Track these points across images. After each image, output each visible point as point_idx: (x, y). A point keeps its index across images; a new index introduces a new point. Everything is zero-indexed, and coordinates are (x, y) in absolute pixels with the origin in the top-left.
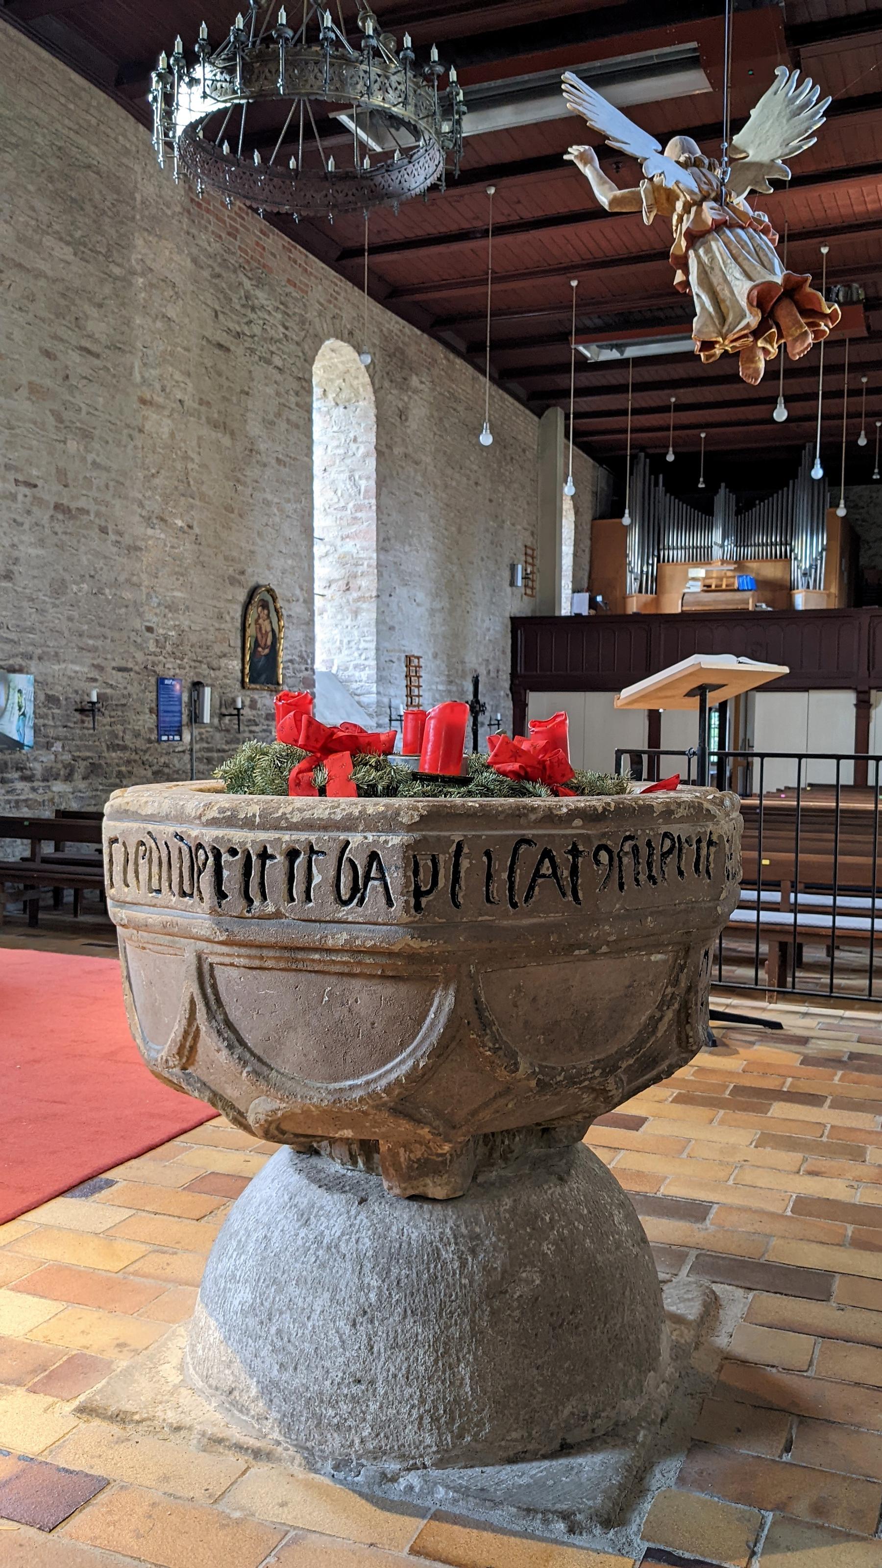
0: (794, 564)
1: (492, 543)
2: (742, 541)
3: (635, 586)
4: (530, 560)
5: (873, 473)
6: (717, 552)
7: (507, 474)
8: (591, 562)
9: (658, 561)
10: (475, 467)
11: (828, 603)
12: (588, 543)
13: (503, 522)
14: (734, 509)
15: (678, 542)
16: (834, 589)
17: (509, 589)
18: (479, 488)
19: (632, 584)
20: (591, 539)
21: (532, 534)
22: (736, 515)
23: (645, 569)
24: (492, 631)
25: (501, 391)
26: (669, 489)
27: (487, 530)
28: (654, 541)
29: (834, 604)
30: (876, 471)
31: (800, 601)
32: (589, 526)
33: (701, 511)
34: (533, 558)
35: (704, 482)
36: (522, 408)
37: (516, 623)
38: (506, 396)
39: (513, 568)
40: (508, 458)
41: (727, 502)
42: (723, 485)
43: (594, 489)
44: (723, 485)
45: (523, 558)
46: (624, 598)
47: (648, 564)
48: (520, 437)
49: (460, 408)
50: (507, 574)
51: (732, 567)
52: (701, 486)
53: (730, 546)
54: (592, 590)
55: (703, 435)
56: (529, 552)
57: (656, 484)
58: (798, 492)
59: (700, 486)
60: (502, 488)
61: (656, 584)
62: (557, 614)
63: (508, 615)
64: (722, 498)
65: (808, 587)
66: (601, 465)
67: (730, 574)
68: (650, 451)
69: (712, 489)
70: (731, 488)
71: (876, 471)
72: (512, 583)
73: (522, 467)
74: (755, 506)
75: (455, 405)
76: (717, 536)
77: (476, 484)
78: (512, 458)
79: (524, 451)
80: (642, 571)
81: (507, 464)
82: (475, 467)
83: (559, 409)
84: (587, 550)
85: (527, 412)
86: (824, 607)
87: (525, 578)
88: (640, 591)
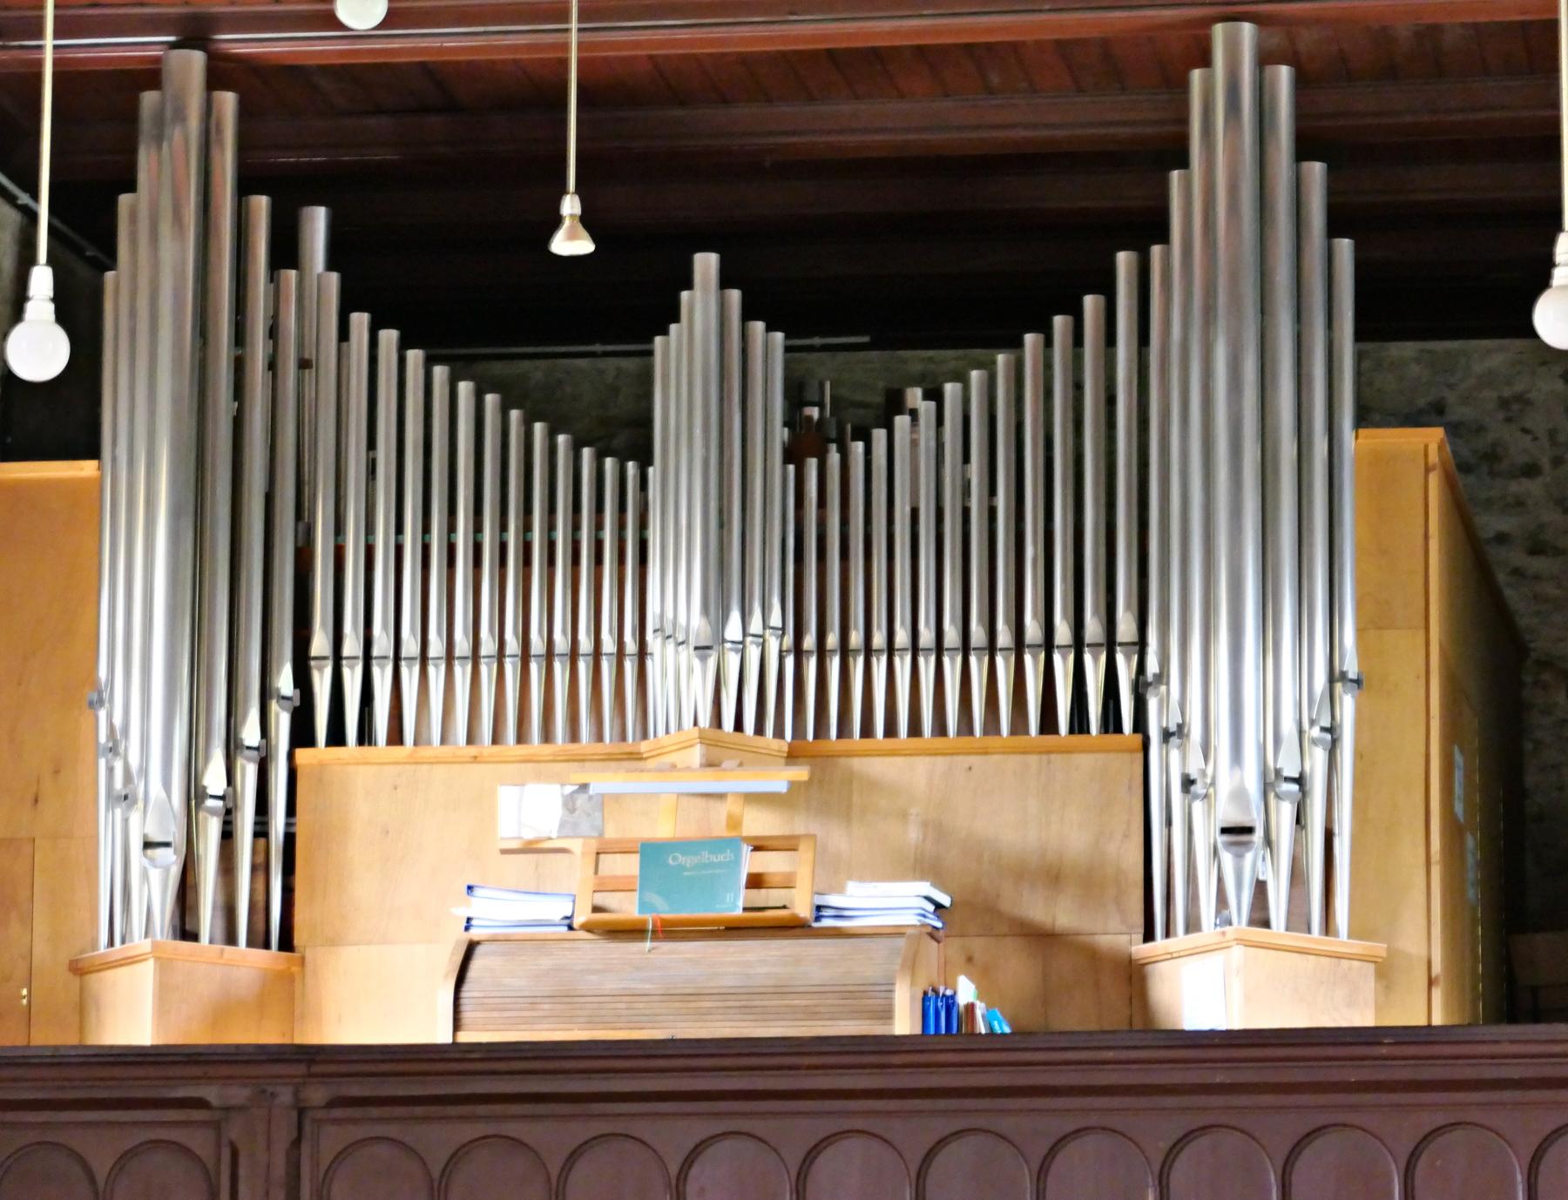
0: (1167, 764)
3: (154, 887)
6: (680, 683)
9: (302, 735)
11: (1379, 1008)
14: (781, 434)
15: (411, 620)
22: (793, 454)
23: (214, 779)
28: (266, 584)
29: (1423, 1005)
31: (1210, 986)
35: (589, 221)
42: (706, 264)
44: (706, 264)
47: (232, 746)
51: (778, 780)
52: (571, 243)
53: (761, 635)
57: (286, 252)
61: (268, 888)
65: (1261, 919)
67: (759, 823)
68: (236, 42)
69: (631, 299)
80: (195, 794)
88: (186, 931)
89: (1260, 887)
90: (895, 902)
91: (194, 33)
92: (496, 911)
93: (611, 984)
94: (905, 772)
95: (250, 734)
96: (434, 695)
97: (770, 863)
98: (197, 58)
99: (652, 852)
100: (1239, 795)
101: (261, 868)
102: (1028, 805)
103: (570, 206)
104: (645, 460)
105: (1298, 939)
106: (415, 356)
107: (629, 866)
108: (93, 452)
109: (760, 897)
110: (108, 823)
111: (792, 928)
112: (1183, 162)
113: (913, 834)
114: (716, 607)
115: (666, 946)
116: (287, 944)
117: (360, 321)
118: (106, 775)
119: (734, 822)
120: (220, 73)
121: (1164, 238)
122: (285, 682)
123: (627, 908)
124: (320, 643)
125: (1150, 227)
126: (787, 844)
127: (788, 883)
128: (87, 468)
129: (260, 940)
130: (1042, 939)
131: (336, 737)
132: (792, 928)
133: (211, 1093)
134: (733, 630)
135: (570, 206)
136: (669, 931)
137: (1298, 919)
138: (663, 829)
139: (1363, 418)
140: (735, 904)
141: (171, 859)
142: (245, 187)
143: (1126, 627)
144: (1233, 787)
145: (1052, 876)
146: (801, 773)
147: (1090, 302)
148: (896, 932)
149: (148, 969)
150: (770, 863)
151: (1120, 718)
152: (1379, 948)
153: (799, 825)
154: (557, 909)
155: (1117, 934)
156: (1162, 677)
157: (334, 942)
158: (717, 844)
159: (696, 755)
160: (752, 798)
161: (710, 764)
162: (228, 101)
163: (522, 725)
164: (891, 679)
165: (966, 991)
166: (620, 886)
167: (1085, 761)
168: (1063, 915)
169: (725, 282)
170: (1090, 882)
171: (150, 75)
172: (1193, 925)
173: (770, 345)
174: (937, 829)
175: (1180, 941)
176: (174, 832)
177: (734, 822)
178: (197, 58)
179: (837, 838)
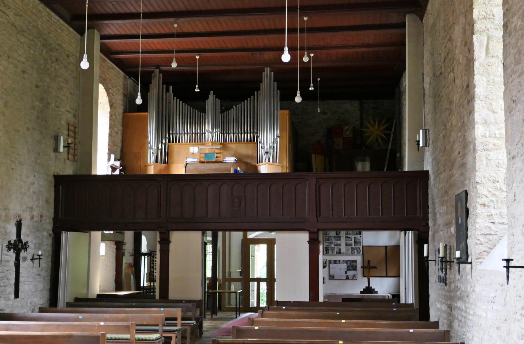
0: (259, 146)
1: (38, 118)
2: (224, 130)
3: (153, 158)
4: (72, 134)
5: (310, 86)
6: (209, 137)
7: (53, 69)
8: (123, 141)
9: (169, 142)
10: (22, 59)
12: (121, 128)
13: (48, 104)
14: (220, 110)
16: (286, 163)
17: (53, 154)
18: (26, 76)
19: (151, 155)
20: (123, 126)
21: (75, 116)
22: (221, 113)
23: (160, 146)
24: (36, 185)
25: (48, 10)
26: (176, 94)
27: (33, 108)
29: (286, 170)
30: (312, 85)
31: (264, 169)
32: (121, 116)
33: (196, 104)
34: (75, 133)
35: (199, 88)
36: (66, 25)
37: (60, 182)
38: (53, 14)
39: (56, 139)
40: (54, 59)
41: (214, 104)
42: (212, 92)
43: (126, 93)
44: (212, 92)
45: (66, 132)
46: (146, 166)
47: (162, 143)
48: (64, 46)
49: (10, 13)
50: (52, 143)
52: (197, 90)
53: (217, 132)
54: (121, 158)
55: (197, 57)
56: (71, 128)
57: (168, 90)
58: (261, 98)
59: (196, 90)
60: (47, 79)
61: (166, 157)
62: (93, 173)
63: (52, 175)
64: (211, 101)
65: (269, 161)
66: (130, 77)
67: (217, 151)
69: (203, 96)
70: (218, 96)
71: (312, 85)
72: (56, 150)
73: (66, 67)
74: (232, 107)
75: (4, 9)
76: (208, 127)
77: (24, 72)
78: (57, 60)
79: (68, 56)
80: (158, 148)
81: (53, 62)
82: (22, 59)
83: (96, 31)
84: (120, 133)
85: (71, 29)
86: (280, 172)
87: (67, 146)
88: (157, 161)
89: (269, 158)
90: (231, 159)
91: (158, 67)
92: (189, 160)
93: (201, 168)
94: (233, 146)
95: (164, 142)
96: (183, 138)
97: (218, 155)
98: (158, 70)
99: (206, 154)
100: (267, 148)
101: (165, 156)
102: (245, 150)
103: (197, 86)
104: (205, 113)
105: (273, 164)
106: (181, 102)
107: (203, 155)
108: (147, 112)
109: (217, 159)
110: (149, 151)
111: (220, 162)
112: (262, 82)
113: (233, 152)
114: (213, 129)
115: (207, 164)
116: (167, 163)
117: (175, 98)
118: (148, 146)
119: (214, 151)
120: (161, 71)
121: (260, 90)
122: (167, 136)
123: (203, 160)
124: (171, 132)
125: (258, 89)
126: (220, 153)
127: (220, 157)
128: (146, 113)
129: (165, 163)
130: (247, 164)
131: (173, 142)
132: (220, 162)
133: (158, 179)
134: (214, 131)
135: (197, 86)
136: (208, 162)
137: (273, 161)
138: (207, 152)
139: (281, 109)
140: (214, 160)
141: (155, 154)
142: (163, 84)
143: (255, 131)
144: (267, 147)
145: (248, 157)
146: (221, 146)
147: (252, 97)
148: (231, 163)
149: (153, 166)
150: (218, 155)
151: (255, 142)
152: (281, 164)
153: (221, 151)
154: (196, 160)
155: (254, 163)
156: (259, 136)
157: (173, 163)
158: (213, 153)
159: (210, 144)
160: (216, 149)
161: (212, 145)
162: (161, 75)
163: (193, 141)
164: (231, 136)
165: (238, 169)
166: (203, 158)
167: (251, 145)
168: (249, 161)
169: (214, 94)
170: (251, 157)
171: (153, 72)
172: (262, 162)
173: (218, 101)
174: (236, 152)
175: (261, 164)
176: (156, 152)
177: (214, 151)
178: (158, 70)
179: (225, 153)
